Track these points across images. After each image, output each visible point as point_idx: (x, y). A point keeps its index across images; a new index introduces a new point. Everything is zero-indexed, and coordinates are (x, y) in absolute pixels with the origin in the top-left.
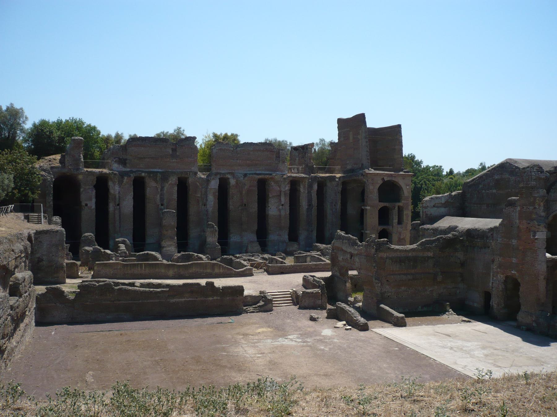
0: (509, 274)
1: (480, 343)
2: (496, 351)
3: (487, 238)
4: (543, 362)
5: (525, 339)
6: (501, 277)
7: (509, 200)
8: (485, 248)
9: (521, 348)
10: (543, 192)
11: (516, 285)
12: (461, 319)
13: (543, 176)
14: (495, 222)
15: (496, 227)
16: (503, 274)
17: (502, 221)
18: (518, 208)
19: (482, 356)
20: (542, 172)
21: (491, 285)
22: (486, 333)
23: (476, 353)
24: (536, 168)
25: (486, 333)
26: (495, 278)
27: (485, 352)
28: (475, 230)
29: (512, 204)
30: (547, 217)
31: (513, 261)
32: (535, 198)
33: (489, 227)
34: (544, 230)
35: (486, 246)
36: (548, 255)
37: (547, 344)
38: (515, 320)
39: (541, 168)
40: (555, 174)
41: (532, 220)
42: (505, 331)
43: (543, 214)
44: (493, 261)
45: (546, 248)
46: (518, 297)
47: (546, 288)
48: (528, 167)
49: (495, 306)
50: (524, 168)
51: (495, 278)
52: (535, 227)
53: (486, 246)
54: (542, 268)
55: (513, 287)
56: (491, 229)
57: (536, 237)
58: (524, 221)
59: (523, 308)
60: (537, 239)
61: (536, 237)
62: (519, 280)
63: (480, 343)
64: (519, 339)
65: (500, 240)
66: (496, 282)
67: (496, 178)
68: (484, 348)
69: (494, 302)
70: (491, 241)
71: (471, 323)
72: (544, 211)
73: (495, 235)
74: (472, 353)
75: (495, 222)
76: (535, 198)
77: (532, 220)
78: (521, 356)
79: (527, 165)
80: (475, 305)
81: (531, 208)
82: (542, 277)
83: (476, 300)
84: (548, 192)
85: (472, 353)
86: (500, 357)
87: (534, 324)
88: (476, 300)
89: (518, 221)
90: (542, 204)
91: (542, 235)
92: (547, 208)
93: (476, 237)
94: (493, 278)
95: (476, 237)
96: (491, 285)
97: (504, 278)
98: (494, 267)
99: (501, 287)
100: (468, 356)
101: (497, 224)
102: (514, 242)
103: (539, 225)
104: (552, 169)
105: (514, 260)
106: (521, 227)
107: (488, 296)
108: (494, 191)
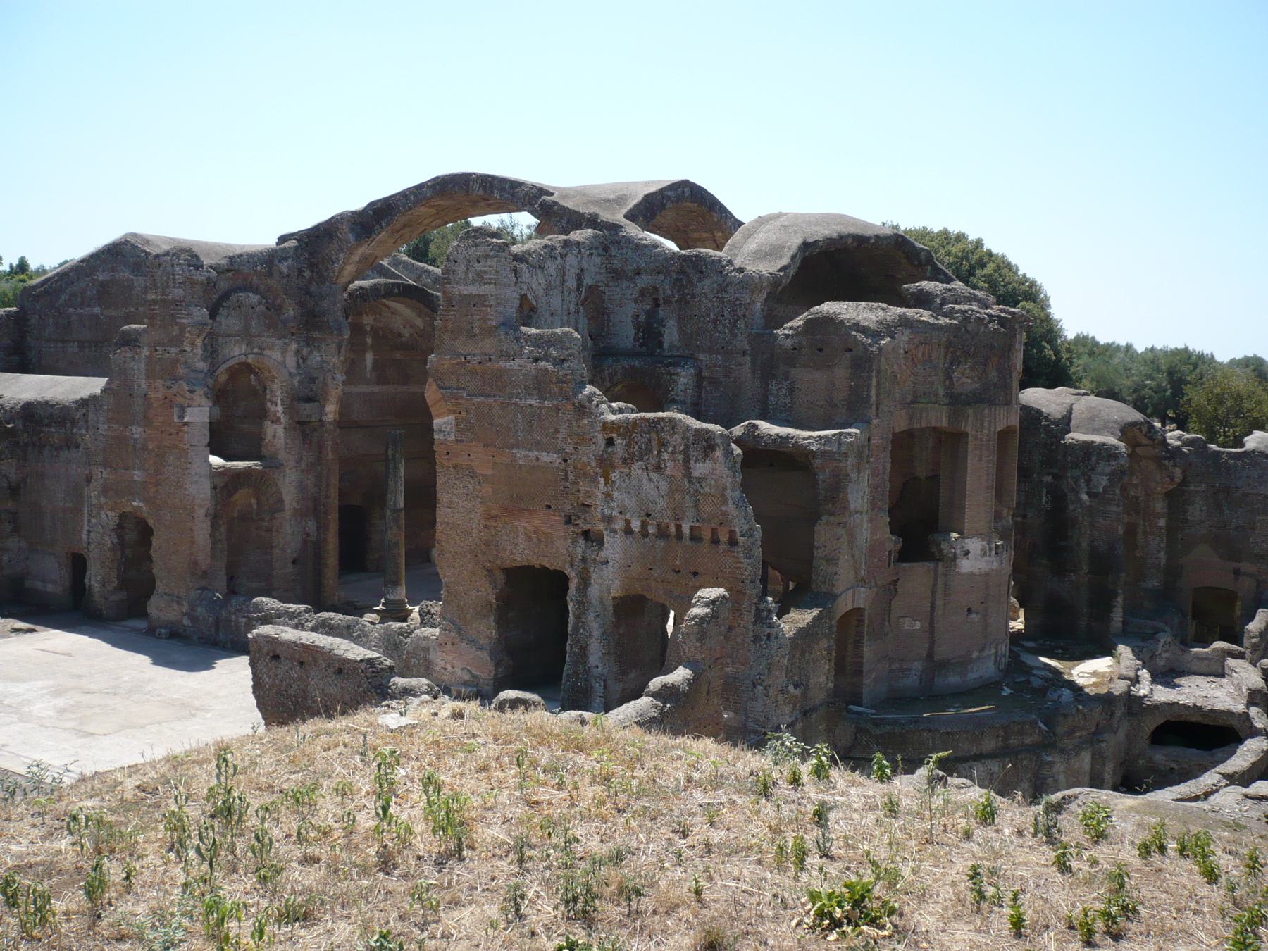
0: (127, 510)
1: (51, 683)
2: (89, 696)
3: (74, 422)
4: (197, 709)
5: (157, 661)
6: (109, 518)
7: (128, 333)
8: (69, 448)
9: (150, 680)
10: (201, 313)
11: (146, 533)
12: (9, 627)
13: (200, 276)
14: (92, 385)
15: (93, 398)
16: (112, 510)
17: (108, 383)
18: (145, 352)
19: (51, 713)
20: (199, 266)
21: (84, 536)
22: (69, 655)
23: (36, 709)
24: (187, 256)
25: (69, 655)
26: (94, 521)
27: (60, 702)
28: (45, 405)
29: (130, 341)
30: (211, 373)
31: (136, 478)
32: (182, 328)
33: (78, 397)
34: (204, 401)
35: (70, 444)
36: (215, 460)
37: (208, 666)
38: (143, 614)
39: (197, 257)
40: (230, 274)
41: (176, 380)
42: (116, 644)
43: (201, 365)
44: (88, 480)
45: (209, 445)
46: (150, 559)
47: (211, 536)
48: (167, 254)
49: (96, 587)
50: (157, 256)
51: (94, 521)
52: (183, 396)
53: (70, 444)
54: (201, 493)
55: (136, 538)
56: (83, 403)
57: (186, 420)
58: (159, 383)
59: (160, 586)
60: (187, 424)
61: (186, 420)
62: (151, 522)
63: (51, 683)
64: (145, 660)
65: (103, 428)
66: (96, 532)
67: (101, 278)
68: (58, 692)
69: (95, 578)
70: (83, 431)
71: (35, 634)
72: (204, 359)
73: (91, 416)
74: (26, 709)
75: (92, 385)
76: (182, 328)
77: (176, 379)
78: (148, 700)
79: (166, 247)
80: (50, 588)
81: (174, 350)
82: (203, 511)
83: (51, 576)
84: (213, 314)
85: (26, 709)
86: (96, 710)
87: (186, 622)
88: (51, 576)
89: (143, 382)
90: (199, 342)
91: (199, 414)
92: (212, 351)
93: (46, 421)
94: (89, 521)
95: (46, 421)
96: (84, 536)
97: (117, 520)
98: (92, 493)
99: (109, 541)
100: (15, 718)
101: (97, 391)
102: (137, 432)
103: (191, 392)
104: (223, 262)
105: (138, 475)
106: (152, 395)
107: (78, 564)
108: (97, 310)
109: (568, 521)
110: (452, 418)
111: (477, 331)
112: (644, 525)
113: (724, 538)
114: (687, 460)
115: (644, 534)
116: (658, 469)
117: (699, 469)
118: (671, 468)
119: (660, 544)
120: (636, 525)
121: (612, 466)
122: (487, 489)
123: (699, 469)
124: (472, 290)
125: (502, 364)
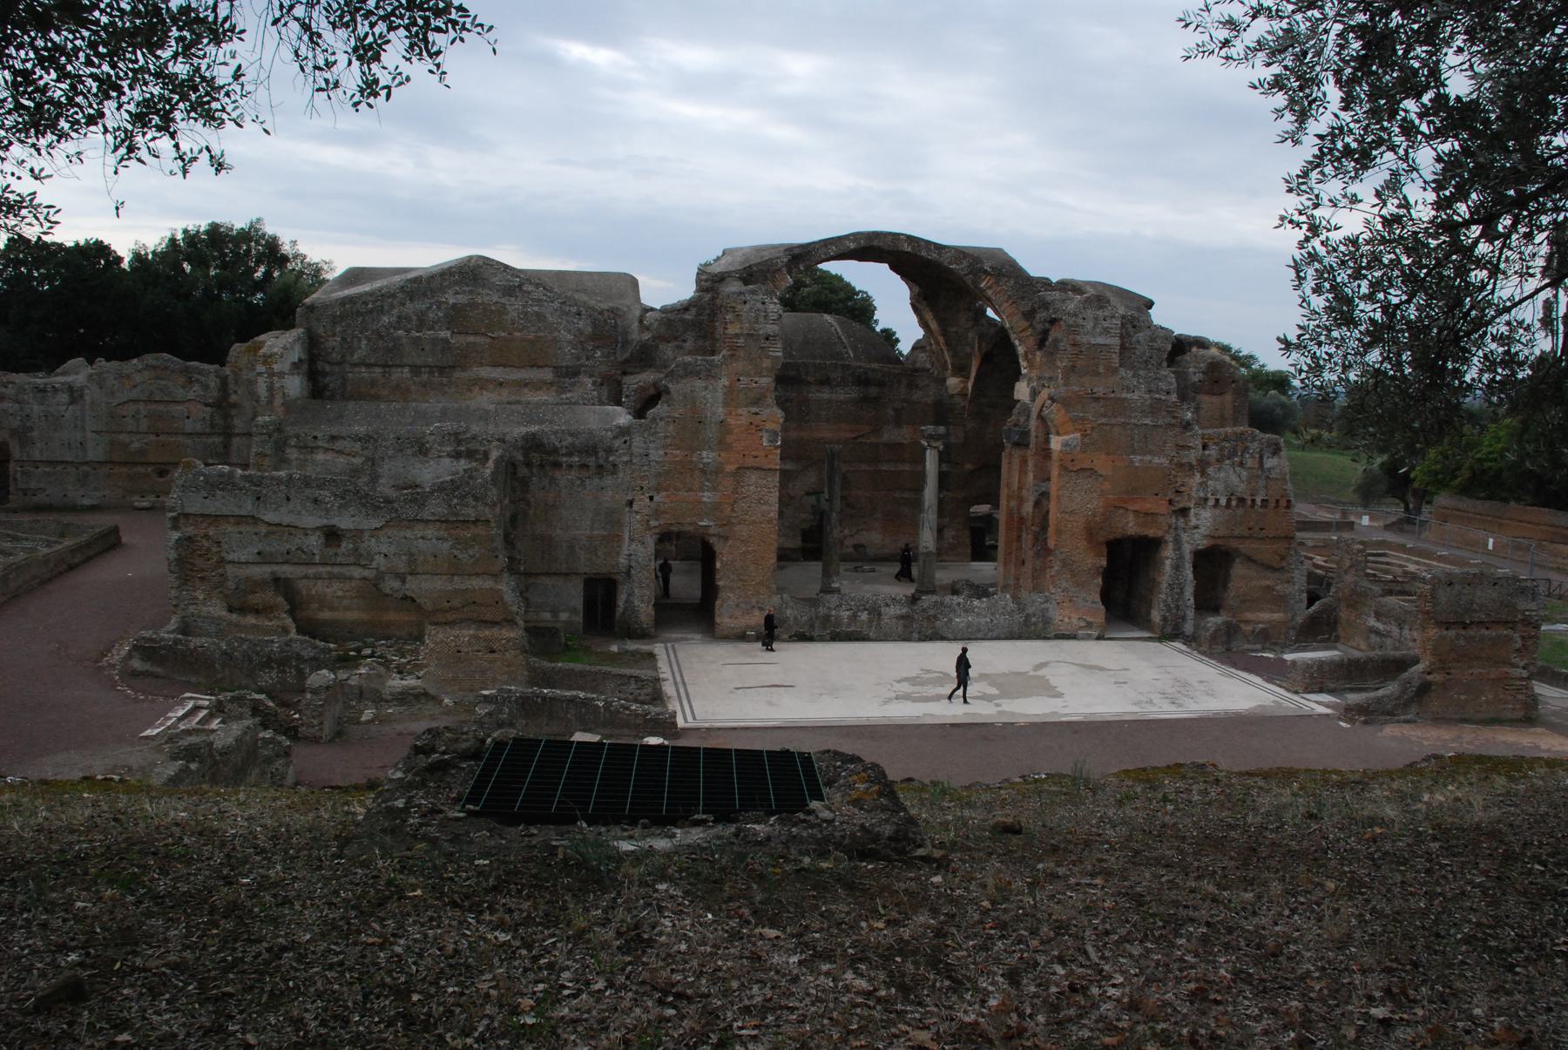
109: (1170, 502)
110: (1078, 435)
111: (1101, 370)
112: (1229, 501)
113: (1283, 503)
114: (1261, 458)
115: (1228, 505)
116: (1241, 464)
117: (1269, 462)
118: (1250, 463)
119: (1240, 511)
120: (1223, 502)
121: (1208, 464)
122: (1107, 486)
123: (1269, 462)
124: (1100, 340)
125: (1124, 395)
